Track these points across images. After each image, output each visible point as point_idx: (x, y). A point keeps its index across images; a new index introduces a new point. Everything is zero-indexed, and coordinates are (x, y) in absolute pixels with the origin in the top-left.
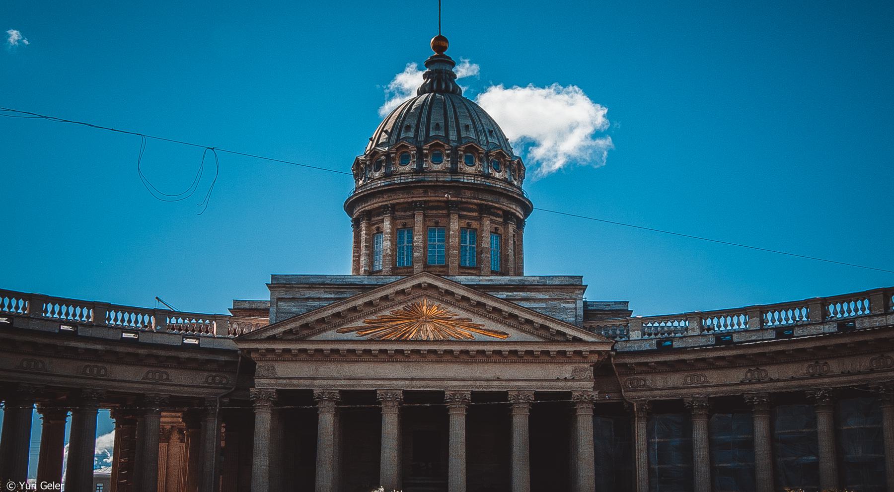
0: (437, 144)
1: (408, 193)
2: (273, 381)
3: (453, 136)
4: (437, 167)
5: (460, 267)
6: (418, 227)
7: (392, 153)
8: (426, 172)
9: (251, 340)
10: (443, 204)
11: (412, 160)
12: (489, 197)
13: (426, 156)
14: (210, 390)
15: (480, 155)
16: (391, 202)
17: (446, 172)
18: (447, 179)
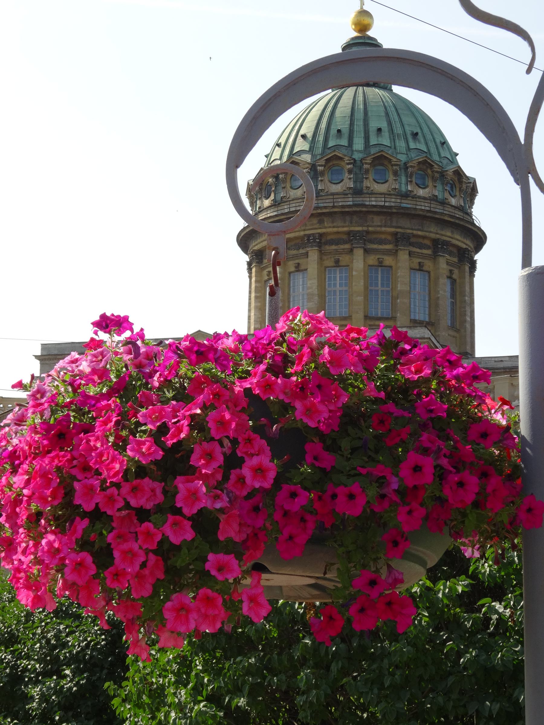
3: (359, 144)
5: (366, 317)
8: (322, 196)
10: (345, 237)
12: (405, 223)
13: (322, 173)
15: (394, 167)
17: (347, 194)
18: (349, 203)
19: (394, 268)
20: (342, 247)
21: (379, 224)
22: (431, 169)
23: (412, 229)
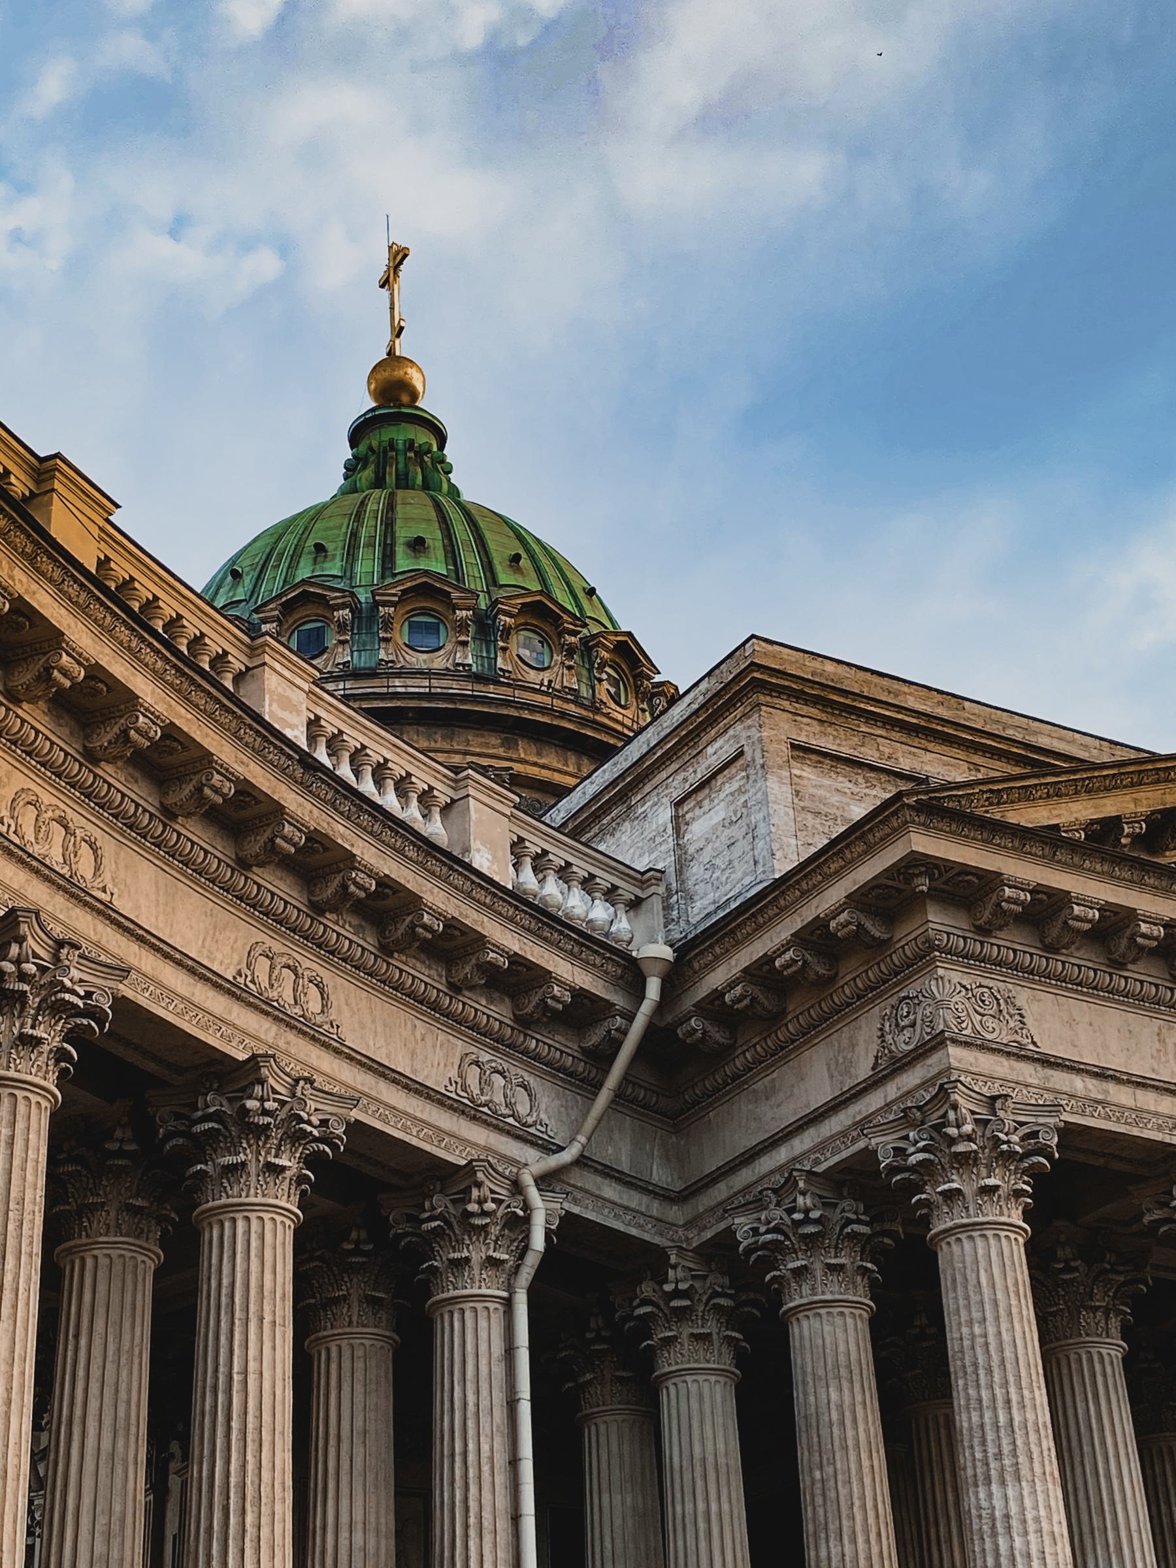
1: (449, 737)
2: (1028, 1072)
7: (385, 604)
13: (507, 632)
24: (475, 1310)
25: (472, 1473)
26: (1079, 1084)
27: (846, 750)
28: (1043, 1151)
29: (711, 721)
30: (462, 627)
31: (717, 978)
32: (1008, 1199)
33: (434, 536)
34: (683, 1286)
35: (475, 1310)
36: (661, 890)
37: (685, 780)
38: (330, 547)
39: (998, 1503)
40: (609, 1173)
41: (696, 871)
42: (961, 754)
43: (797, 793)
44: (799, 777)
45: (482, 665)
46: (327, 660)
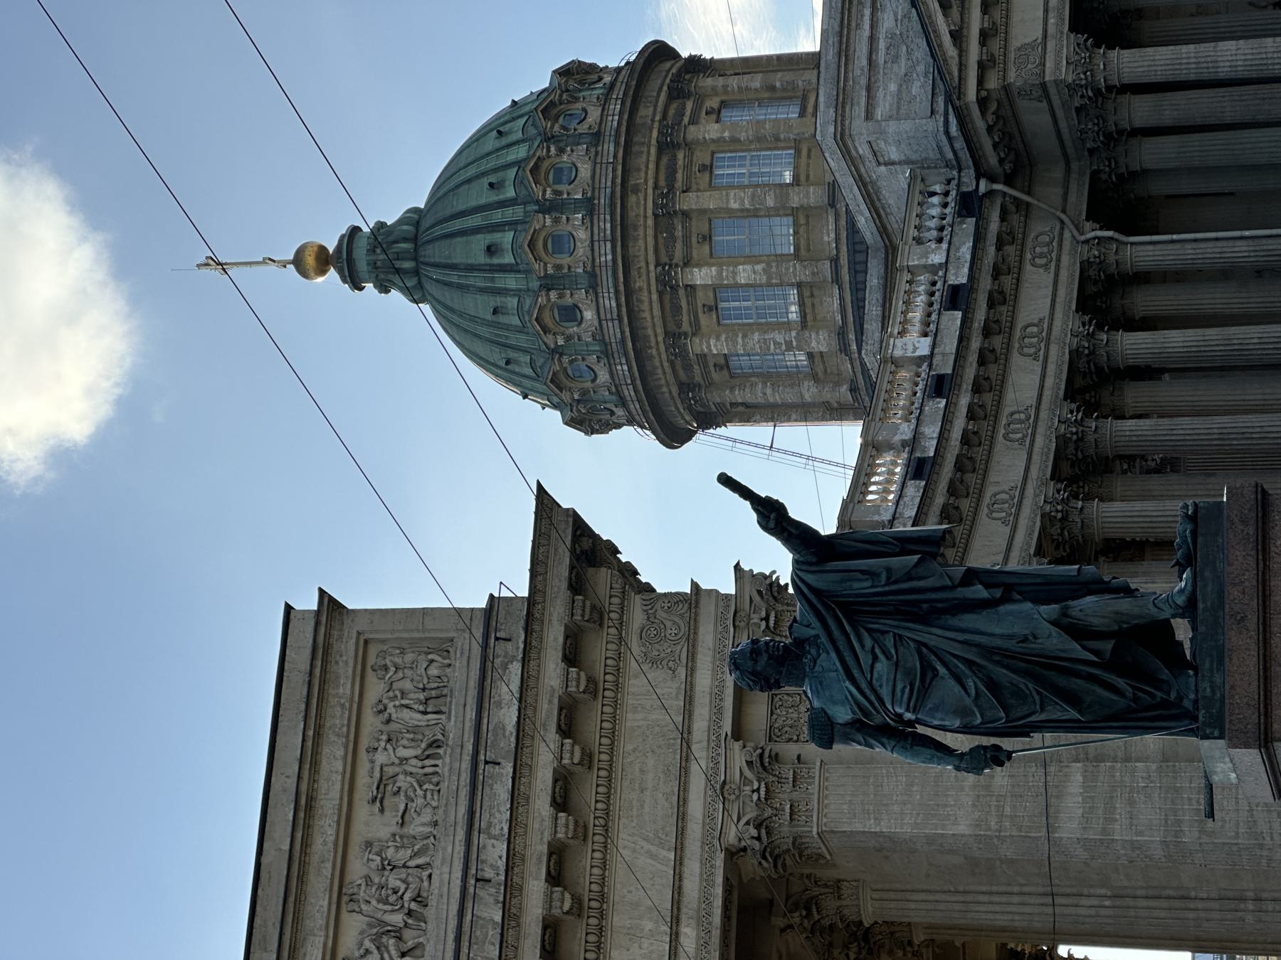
0: (535, 170)
1: (636, 229)
2: (1051, 45)
3: (521, 152)
4: (585, 171)
6: (710, 201)
7: (546, 270)
9: (960, 71)
10: (665, 160)
11: (564, 228)
14: (1065, 259)
16: (652, 267)
17: (597, 153)
19: (724, 98)
20: (680, 163)
21: (651, 109)
22: (573, 75)
23: (666, 76)
24: (1135, 257)
25: (1200, 256)
26: (1052, 21)
27: (864, 93)
28: (1086, 41)
29: (849, 152)
30: (556, 221)
31: (993, 160)
32: (1106, 57)
33: (482, 241)
34: (1107, 163)
35: (1135, 257)
36: (918, 171)
37: (870, 161)
38: (493, 304)
39: (1225, 69)
40: (1065, 198)
41: (914, 157)
42: (852, 33)
43: (890, 117)
44: (882, 115)
45: (581, 207)
46: (583, 303)
